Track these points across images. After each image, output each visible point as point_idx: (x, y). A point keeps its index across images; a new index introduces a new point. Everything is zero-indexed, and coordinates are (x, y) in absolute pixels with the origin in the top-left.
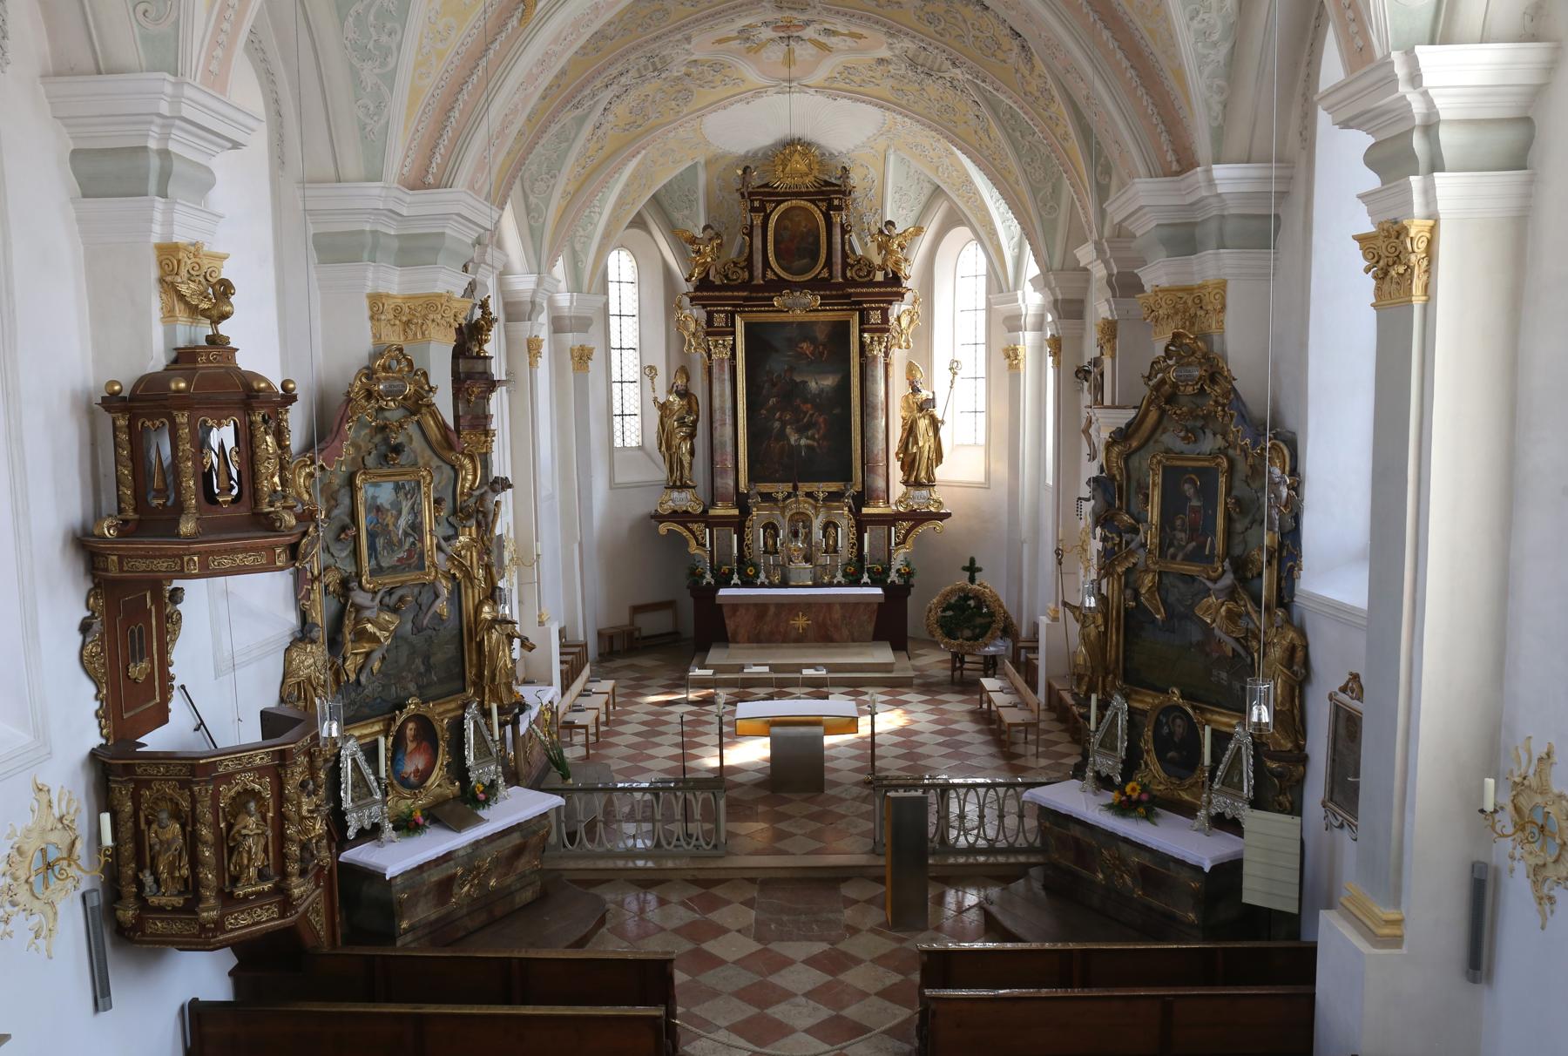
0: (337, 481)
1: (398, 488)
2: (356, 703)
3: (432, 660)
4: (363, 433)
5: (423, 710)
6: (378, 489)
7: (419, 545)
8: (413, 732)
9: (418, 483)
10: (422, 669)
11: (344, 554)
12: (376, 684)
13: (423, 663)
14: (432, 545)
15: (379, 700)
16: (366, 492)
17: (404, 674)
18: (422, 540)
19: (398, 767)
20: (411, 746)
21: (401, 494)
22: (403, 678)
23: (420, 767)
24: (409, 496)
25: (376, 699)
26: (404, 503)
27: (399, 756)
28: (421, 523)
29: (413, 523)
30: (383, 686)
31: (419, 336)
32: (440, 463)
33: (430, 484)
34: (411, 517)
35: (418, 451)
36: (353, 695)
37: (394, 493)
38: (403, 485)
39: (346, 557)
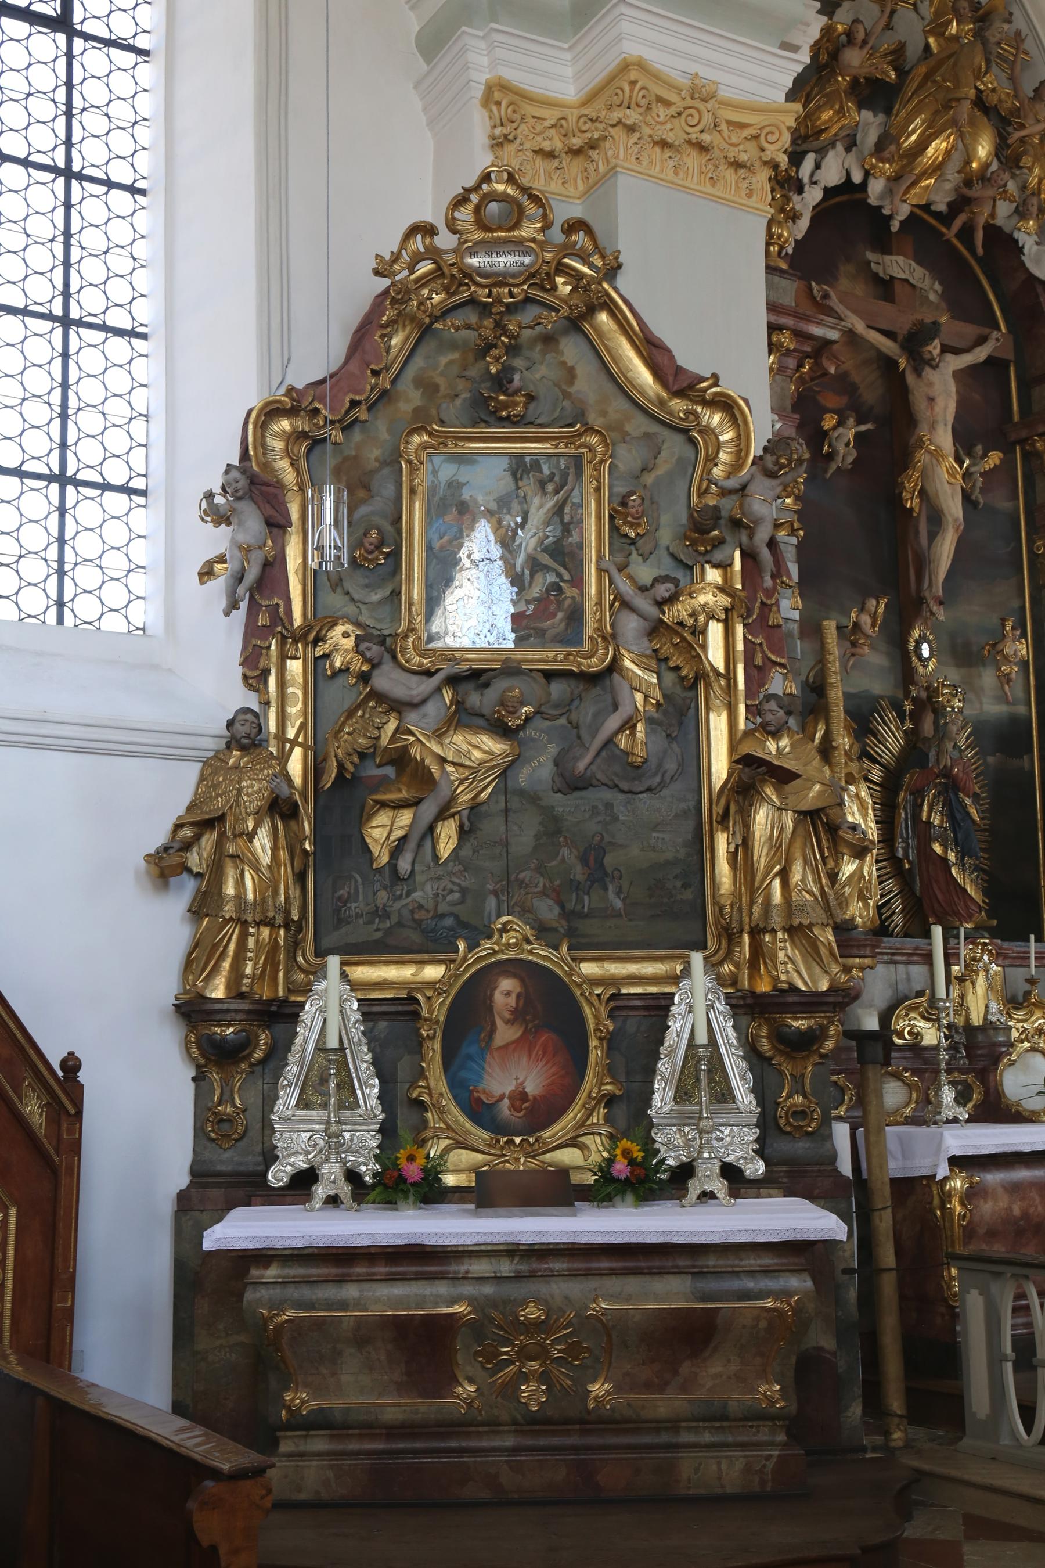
0: (373, 454)
1: (519, 467)
2: (387, 915)
3: (609, 860)
4: (443, 360)
5: (540, 953)
6: (464, 469)
7: (570, 592)
8: (512, 1001)
9: (577, 461)
10: (579, 873)
11: (375, 597)
12: (445, 883)
13: (584, 860)
14: (600, 592)
15: (449, 922)
16: (435, 472)
17: (526, 875)
18: (578, 582)
19: (463, 1074)
20: (505, 1033)
21: (529, 485)
22: (521, 884)
23: (533, 1087)
24: (550, 487)
25: (443, 916)
26: (536, 501)
27: (469, 1048)
28: (581, 546)
29: (558, 542)
30: (463, 891)
31: (602, 169)
32: (655, 428)
33: (602, 461)
34: (552, 533)
35: (591, 398)
36: (383, 896)
37: (509, 479)
38: (536, 466)
39: (380, 602)
